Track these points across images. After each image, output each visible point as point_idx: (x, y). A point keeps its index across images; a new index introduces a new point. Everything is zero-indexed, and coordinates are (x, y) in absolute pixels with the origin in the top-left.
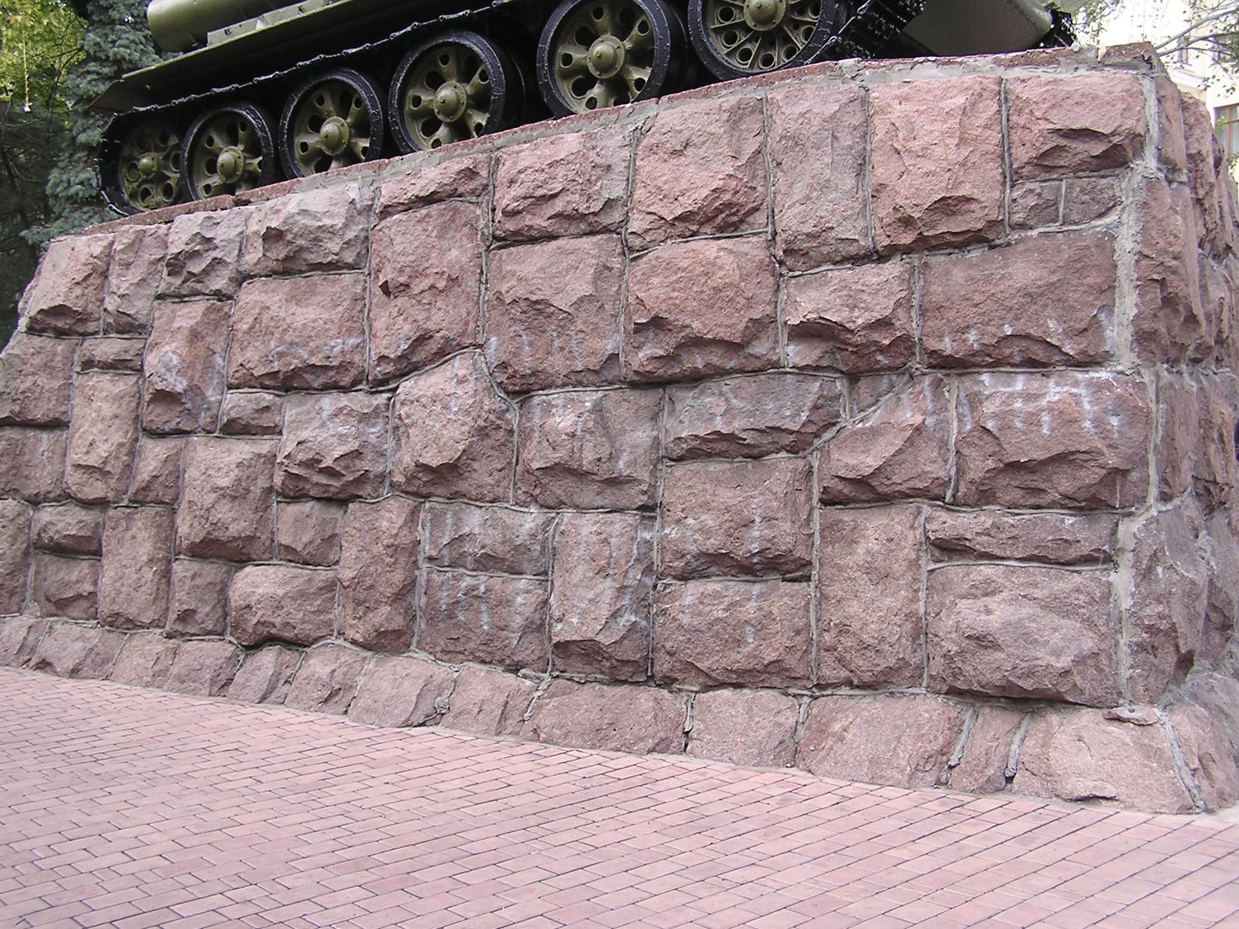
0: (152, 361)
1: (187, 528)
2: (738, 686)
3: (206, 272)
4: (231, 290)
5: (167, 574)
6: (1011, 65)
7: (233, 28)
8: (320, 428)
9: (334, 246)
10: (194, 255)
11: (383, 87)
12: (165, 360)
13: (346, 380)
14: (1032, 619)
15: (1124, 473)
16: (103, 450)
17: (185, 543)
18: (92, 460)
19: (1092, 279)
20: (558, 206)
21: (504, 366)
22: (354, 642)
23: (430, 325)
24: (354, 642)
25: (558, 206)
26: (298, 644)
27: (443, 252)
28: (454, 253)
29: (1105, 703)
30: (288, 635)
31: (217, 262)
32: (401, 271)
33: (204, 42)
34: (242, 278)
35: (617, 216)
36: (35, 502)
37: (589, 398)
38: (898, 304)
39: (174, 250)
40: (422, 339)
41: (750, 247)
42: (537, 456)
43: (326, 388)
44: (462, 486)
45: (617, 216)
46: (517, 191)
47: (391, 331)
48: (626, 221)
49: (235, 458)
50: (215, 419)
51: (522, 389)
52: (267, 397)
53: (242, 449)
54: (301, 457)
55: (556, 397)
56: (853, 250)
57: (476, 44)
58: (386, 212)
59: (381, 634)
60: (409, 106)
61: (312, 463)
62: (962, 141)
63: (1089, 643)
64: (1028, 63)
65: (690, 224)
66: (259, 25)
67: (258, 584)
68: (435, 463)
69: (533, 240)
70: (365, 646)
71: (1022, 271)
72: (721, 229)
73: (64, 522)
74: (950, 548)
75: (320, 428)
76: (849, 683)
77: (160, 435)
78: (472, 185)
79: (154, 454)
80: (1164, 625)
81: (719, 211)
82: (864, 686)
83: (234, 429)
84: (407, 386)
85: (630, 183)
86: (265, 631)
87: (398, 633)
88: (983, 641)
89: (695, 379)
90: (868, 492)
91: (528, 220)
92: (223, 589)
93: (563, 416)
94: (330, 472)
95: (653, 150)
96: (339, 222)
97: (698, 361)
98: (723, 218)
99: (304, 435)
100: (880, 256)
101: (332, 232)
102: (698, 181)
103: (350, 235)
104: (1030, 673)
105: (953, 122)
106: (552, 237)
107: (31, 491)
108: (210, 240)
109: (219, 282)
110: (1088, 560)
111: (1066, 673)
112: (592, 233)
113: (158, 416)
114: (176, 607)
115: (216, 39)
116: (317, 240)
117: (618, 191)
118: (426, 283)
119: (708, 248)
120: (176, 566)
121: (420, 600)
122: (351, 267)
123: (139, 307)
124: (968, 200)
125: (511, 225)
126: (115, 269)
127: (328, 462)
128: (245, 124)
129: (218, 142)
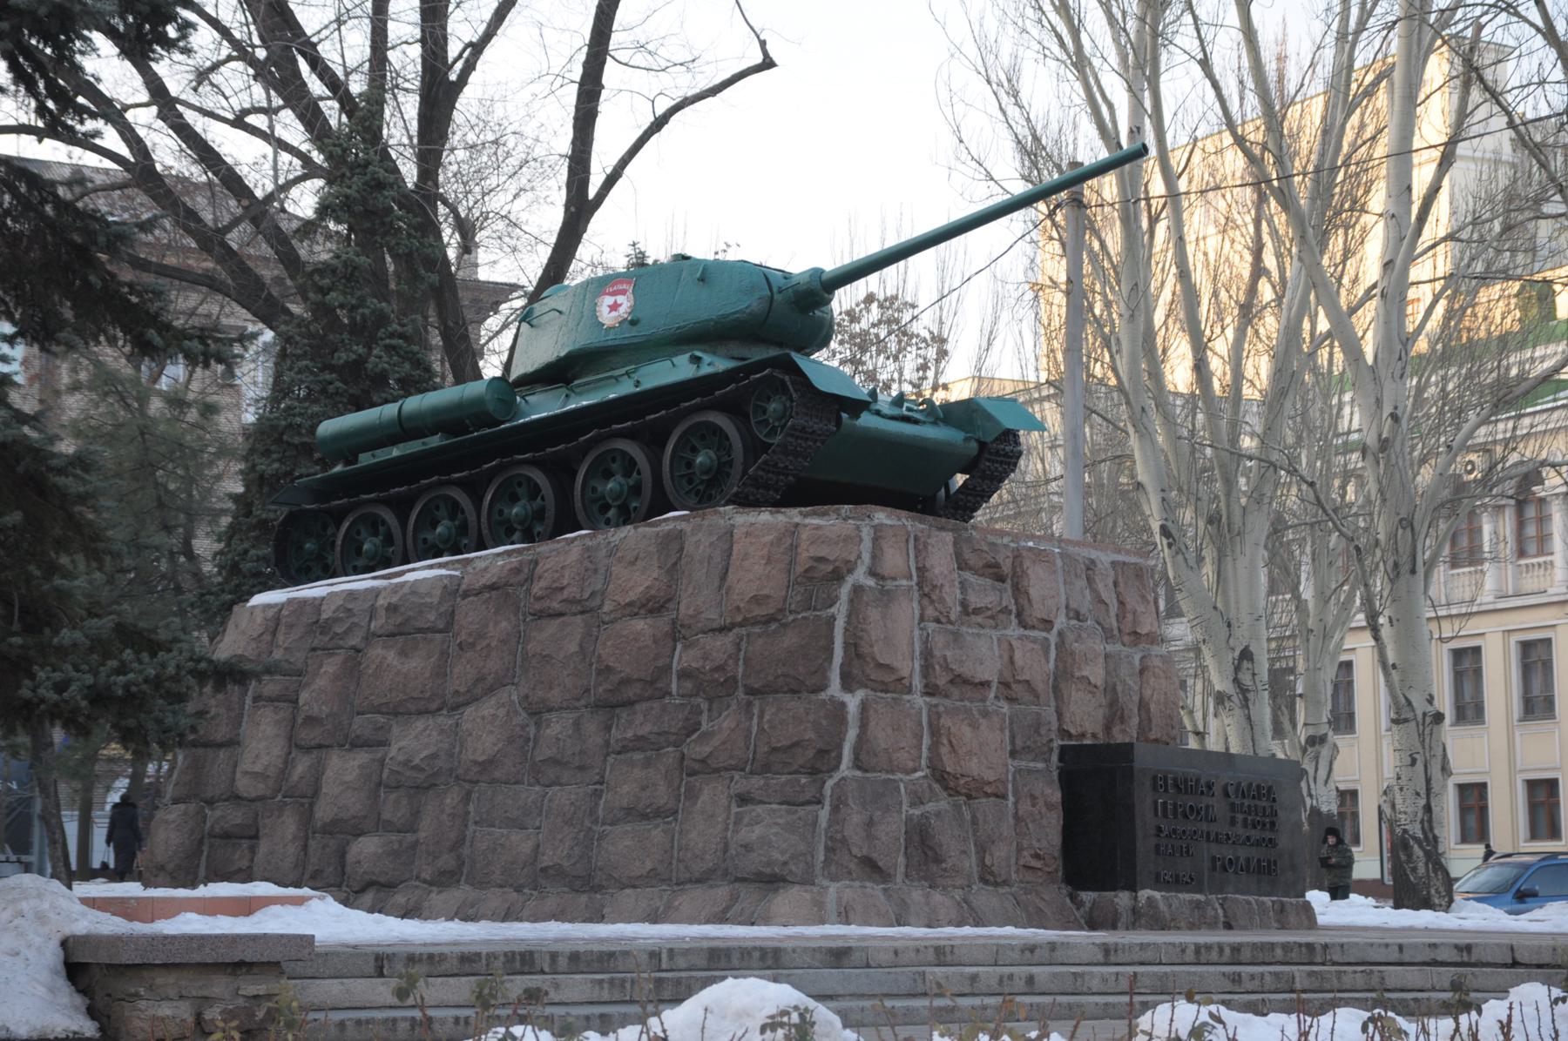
0: (304, 696)
1: (324, 812)
2: (634, 887)
3: (345, 632)
4: (362, 646)
5: (305, 847)
6: (805, 516)
7: (378, 452)
8: (414, 741)
9: (432, 617)
10: (337, 620)
11: (477, 501)
12: (316, 695)
13: (434, 706)
14: (776, 834)
15: (827, 752)
16: (265, 760)
17: (319, 824)
18: (258, 768)
19: (822, 643)
20: (566, 594)
21: (527, 697)
22: (425, 881)
23: (485, 671)
24: (425, 881)
25: (566, 594)
26: (390, 886)
27: (497, 623)
28: (504, 624)
29: (807, 881)
30: (382, 880)
31: (354, 625)
32: (470, 635)
33: (356, 461)
34: (370, 637)
35: (597, 602)
36: (210, 802)
37: (570, 717)
38: (730, 656)
39: (324, 616)
40: (480, 679)
41: (663, 623)
42: (544, 752)
43: (420, 713)
44: (497, 774)
45: (597, 602)
46: (543, 583)
47: (462, 673)
48: (601, 606)
49: (356, 763)
50: (346, 736)
51: (538, 712)
52: (381, 719)
53: (362, 757)
54: (401, 758)
55: (553, 716)
56: (715, 625)
57: (539, 477)
58: (466, 595)
59: (442, 873)
60: (496, 517)
61: (406, 763)
62: (769, 561)
63: (802, 847)
64: (815, 514)
65: (636, 609)
66: (396, 452)
67: (366, 848)
68: (481, 759)
69: (551, 616)
70: (431, 884)
71: (790, 640)
72: (651, 612)
73: (230, 816)
74: (743, 799)
75: (414, 741)
76: (690, 881)
77: (308, 749)
78: (521, 577)
79: (302, 765)
80: (839, 836)
81: (649, 601)
82: (699, 881)
83: (357, 744)
84: (469, 711)
85: (607, 581)
86: (367, 877)
87: (452, 873)
88: (747, 847)
89: (629, 704)
90: (705, 768)
91: (545, 604)
92: (342, 854)
93: (557, 726)
94: (417, 768)
95: (620, 560)
96: (436, 600)
97: (631, 692)
98: (653, 606)
99: (401, 744)
100: (723, 629)
101: (430, 606)
102: (639, 581)
103: (442, 609)
104: (768, 864)
105: (765, 551)
106: (561, 614)
107: (209, 795)
108: (349, 610)
109: (355, 641)
110: (809, 803)
111: (785, 863)
112: (582, 613)
113: (309, 735)
114: (310, 868)
115: (365, 459)
116: (421, 612)
117: (599, 587)
118: (485, 643)
119: (640, 624)
120: (312, 843)
121: (466, 851)
122: (440, 631)
123: (298, 658)
124: (768, 597)
125: (537, 606)
126: (282, 629)
127: (417, 761)
128: (384, 522)
129: (364, 533)
